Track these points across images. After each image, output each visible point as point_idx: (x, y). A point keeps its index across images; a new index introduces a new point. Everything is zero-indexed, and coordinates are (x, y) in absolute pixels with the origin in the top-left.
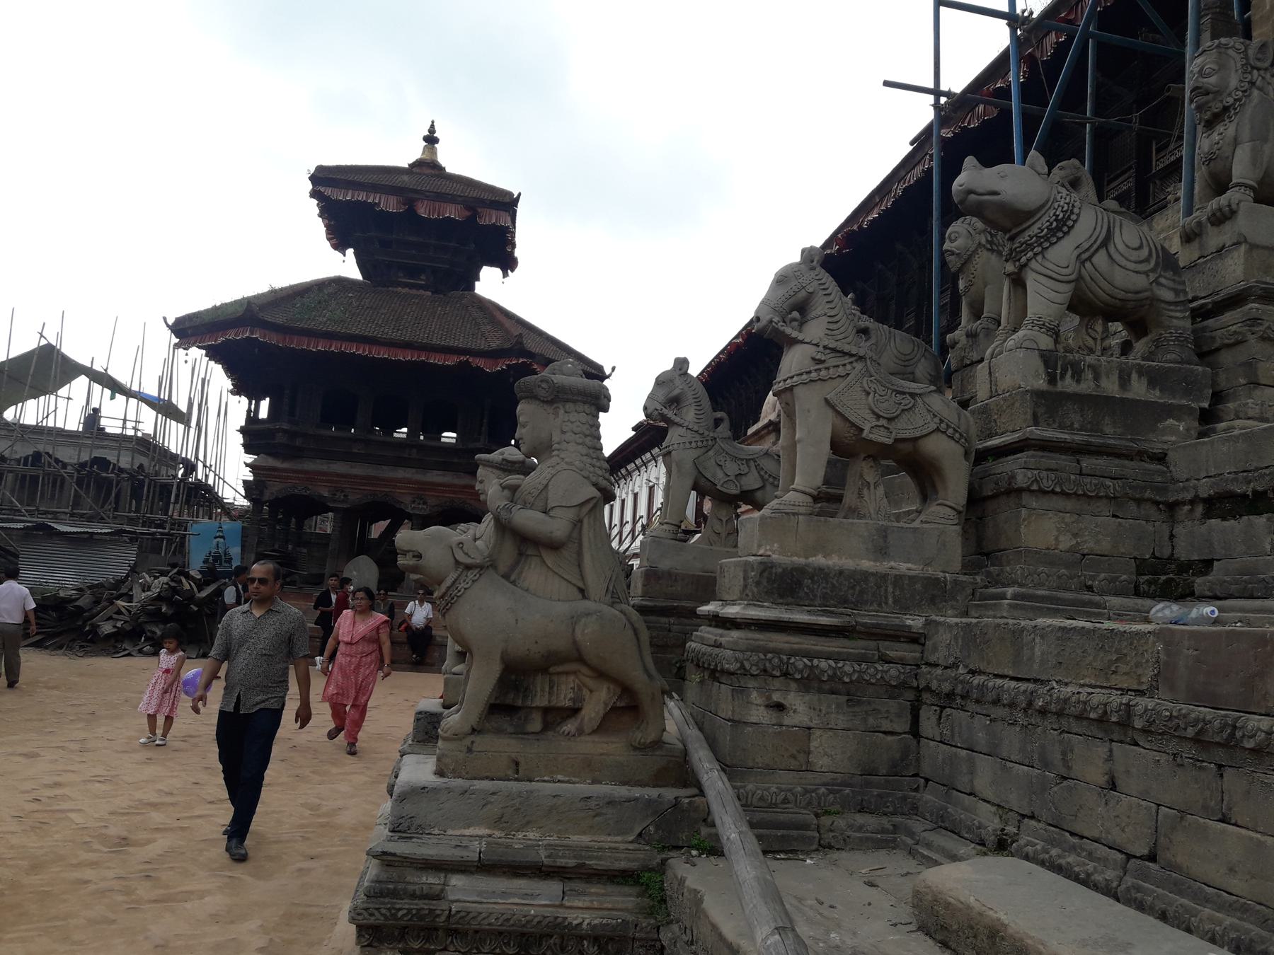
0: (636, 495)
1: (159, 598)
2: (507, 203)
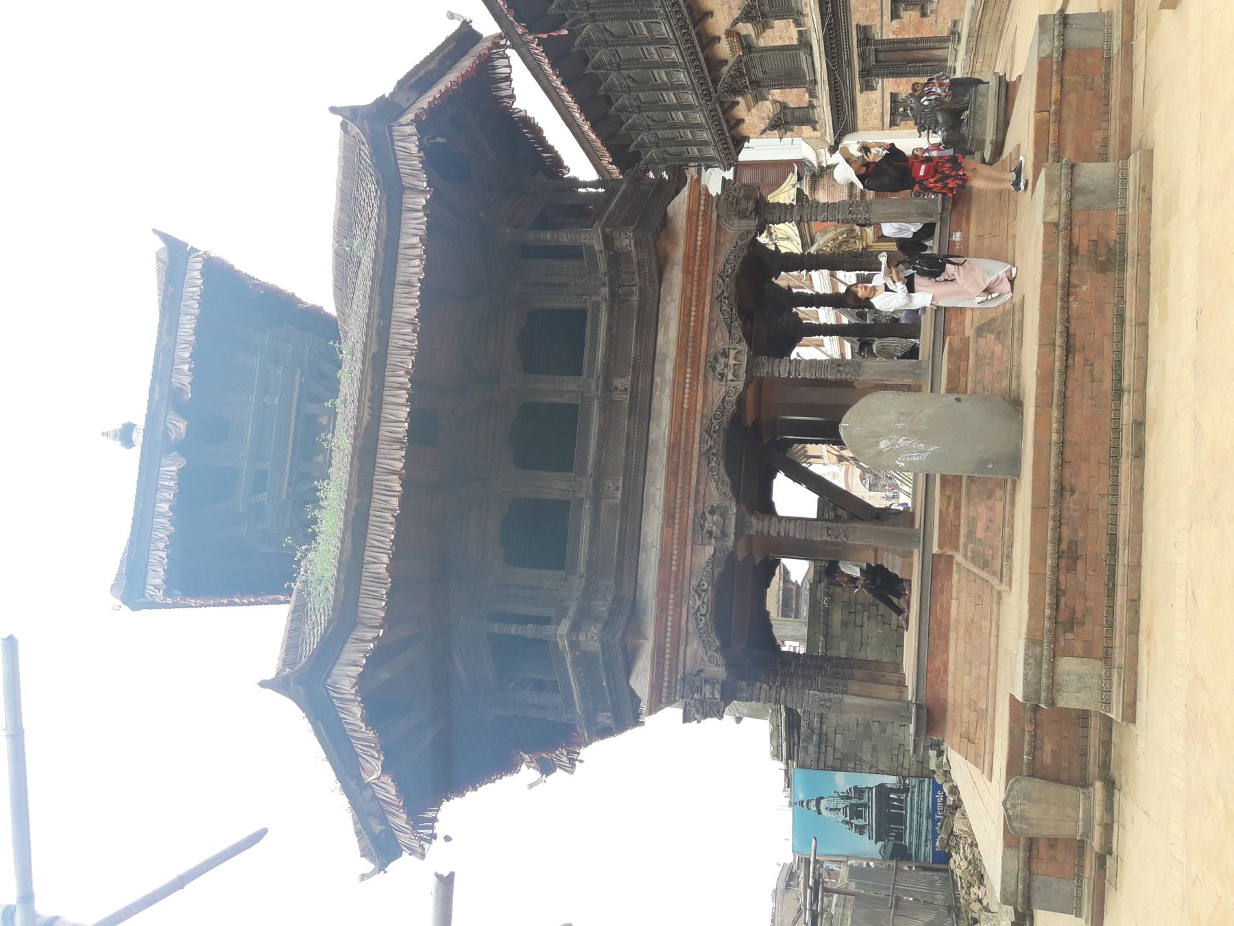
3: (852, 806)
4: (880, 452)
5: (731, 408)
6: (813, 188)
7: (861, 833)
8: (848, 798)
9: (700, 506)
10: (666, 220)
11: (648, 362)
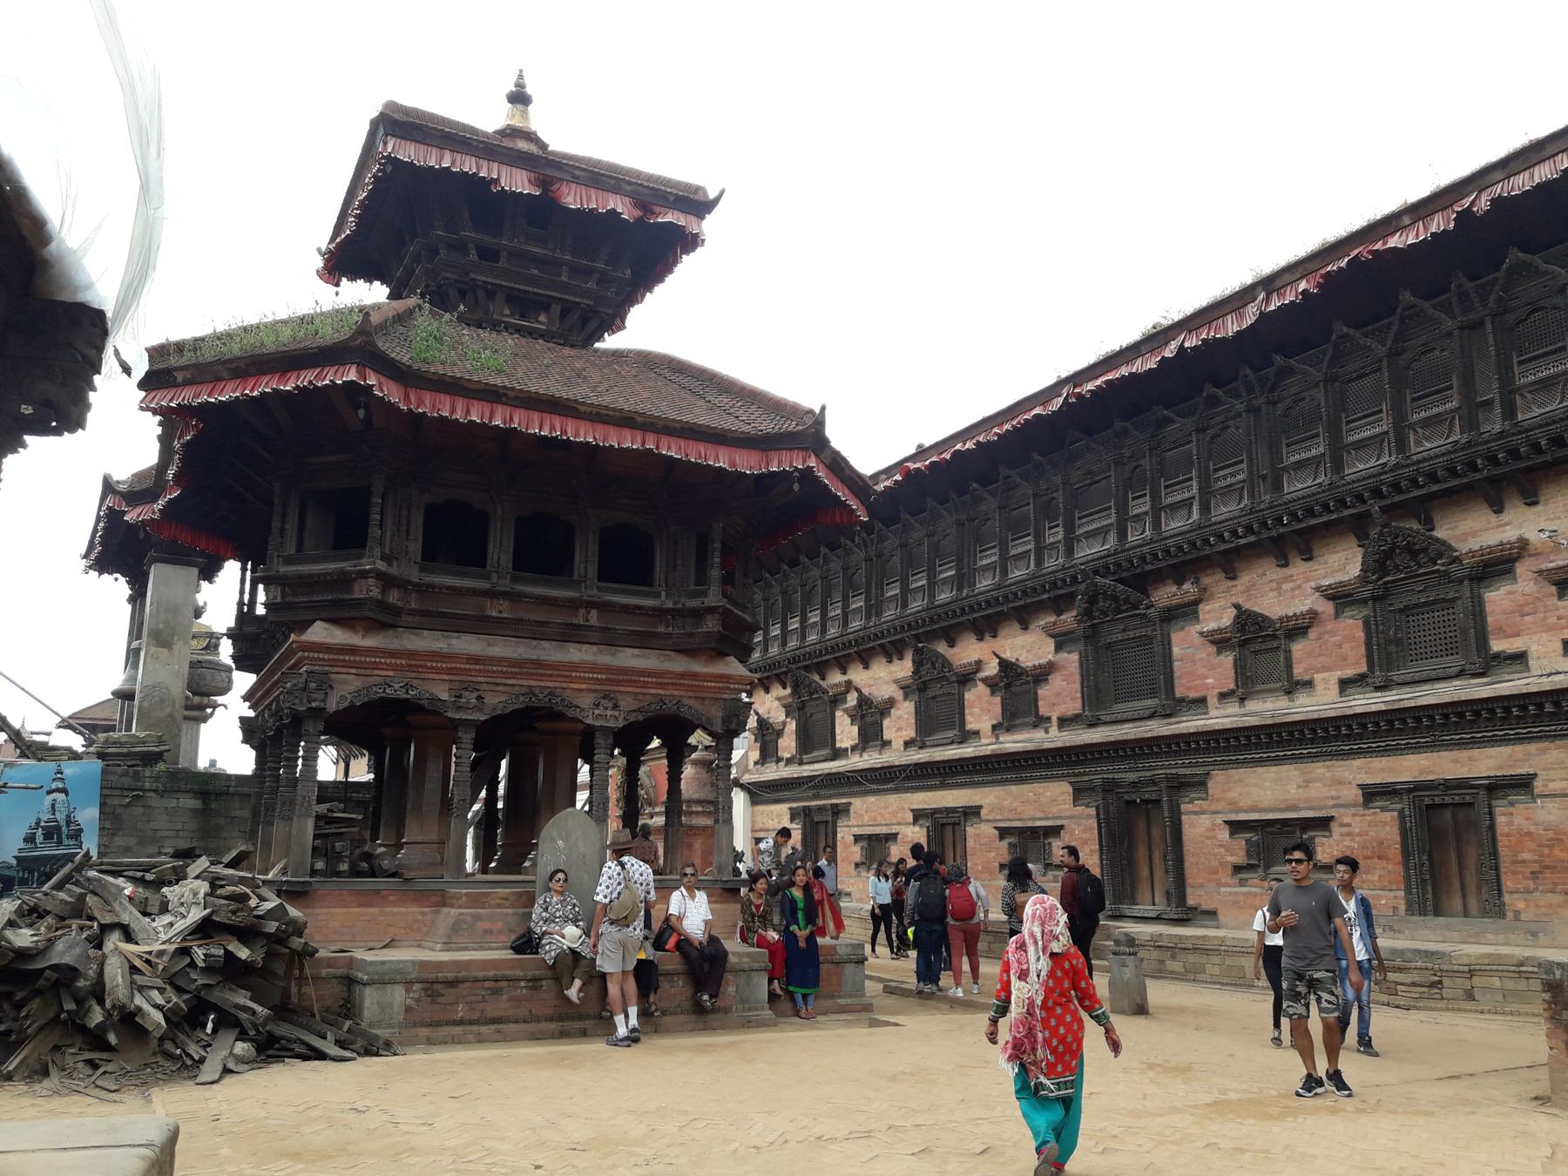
1: (205, 929)
2: (699, 205)
3: (58, 828)
4: (554, 841)
5: (570, 713)
7: (26, 840)
8: (68, 823)
9: (485, 687)
10: (720, 654)
11: (610, 640)
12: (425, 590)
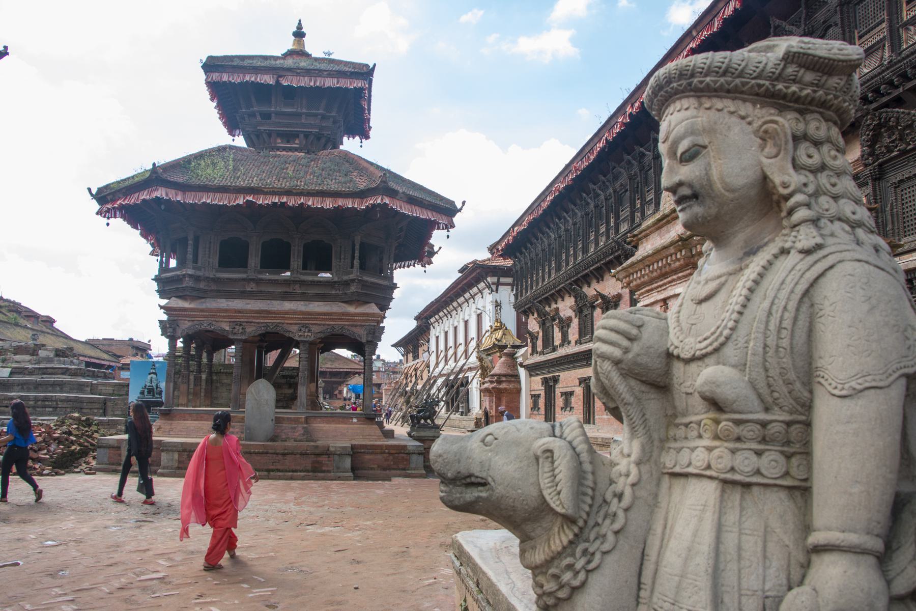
0: (466, 322)
2: (365, 73)
3: (153, 389)
5: (287, 335)
6: (507, 355)
12: (217, 281)
